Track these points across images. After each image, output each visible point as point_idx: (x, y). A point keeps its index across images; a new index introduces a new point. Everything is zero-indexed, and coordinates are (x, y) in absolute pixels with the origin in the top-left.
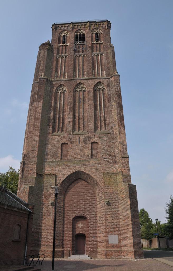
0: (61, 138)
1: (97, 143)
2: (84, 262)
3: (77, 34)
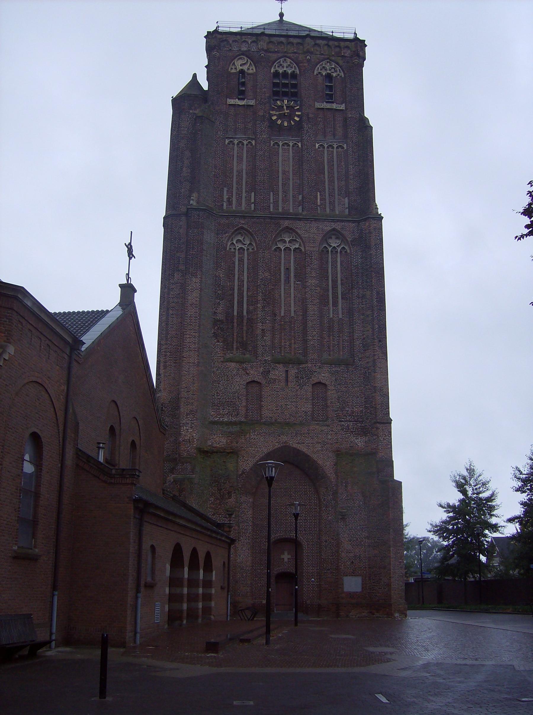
0: (245, 369)
1: (325, 385)
2: (518, 529)
3: (276, 71)
